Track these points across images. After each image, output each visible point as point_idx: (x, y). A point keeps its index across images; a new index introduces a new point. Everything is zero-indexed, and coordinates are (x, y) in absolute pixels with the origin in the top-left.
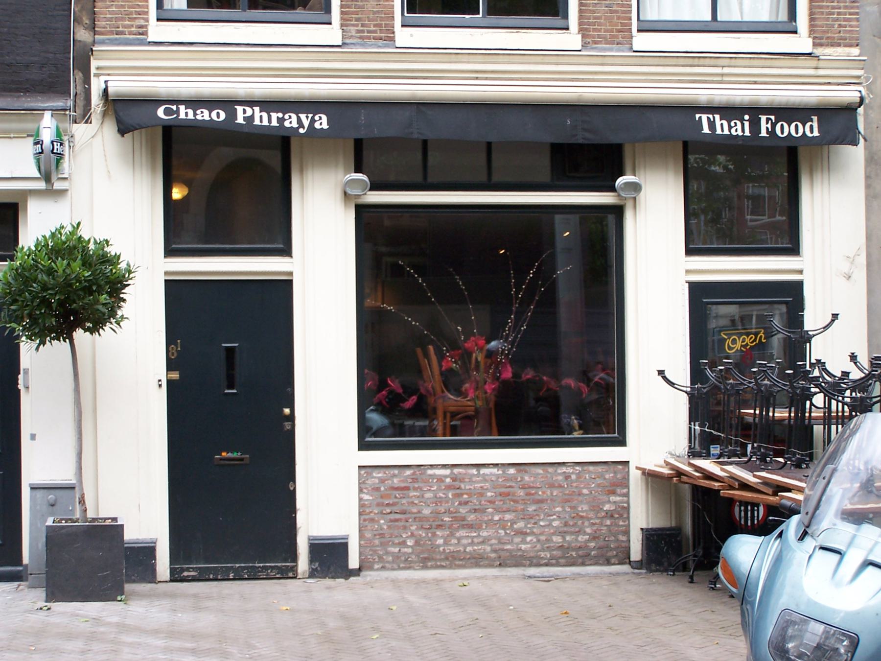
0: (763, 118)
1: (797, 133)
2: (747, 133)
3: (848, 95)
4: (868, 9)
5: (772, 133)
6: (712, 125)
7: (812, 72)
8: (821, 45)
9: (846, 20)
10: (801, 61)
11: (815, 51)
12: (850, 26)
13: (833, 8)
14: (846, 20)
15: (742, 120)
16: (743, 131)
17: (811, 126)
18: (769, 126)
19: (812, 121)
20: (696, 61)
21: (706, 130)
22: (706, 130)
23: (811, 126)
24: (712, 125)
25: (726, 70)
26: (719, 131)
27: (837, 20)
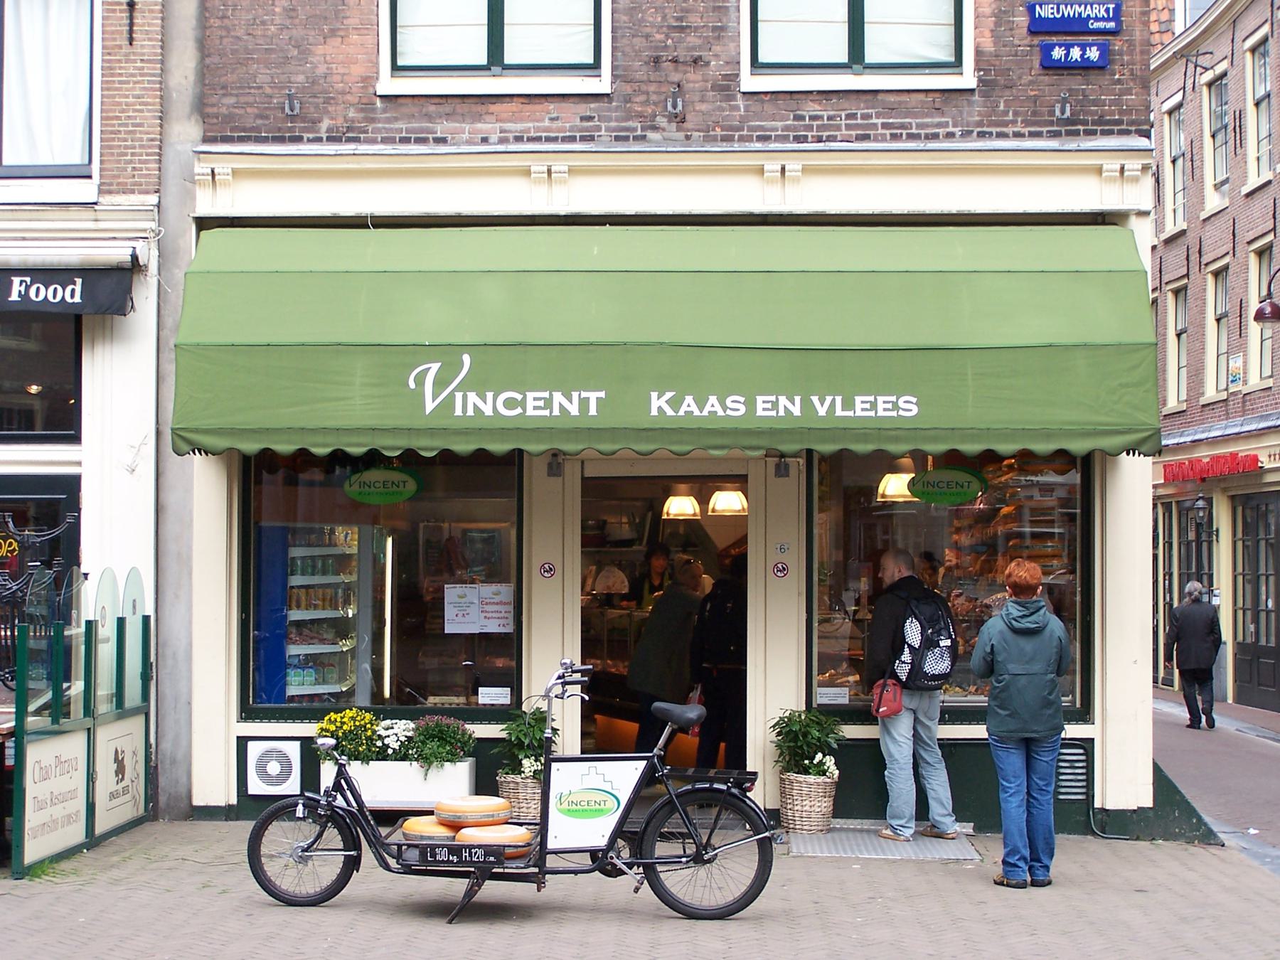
0: (16, 280)
1: (54, 297)
4: (179, 148)
5: (25, 296)
7: (91, 225)
8: (110, 192)
9: (141, 162)
10: (74, 213)
11: (101, 200)
12: (147, 169)
13: (126, 147)
14: (141, 162)
17: (73, 291)
18: (23, 289)
19: (74, 283)
23: (73, 291)
27: (131, 162)
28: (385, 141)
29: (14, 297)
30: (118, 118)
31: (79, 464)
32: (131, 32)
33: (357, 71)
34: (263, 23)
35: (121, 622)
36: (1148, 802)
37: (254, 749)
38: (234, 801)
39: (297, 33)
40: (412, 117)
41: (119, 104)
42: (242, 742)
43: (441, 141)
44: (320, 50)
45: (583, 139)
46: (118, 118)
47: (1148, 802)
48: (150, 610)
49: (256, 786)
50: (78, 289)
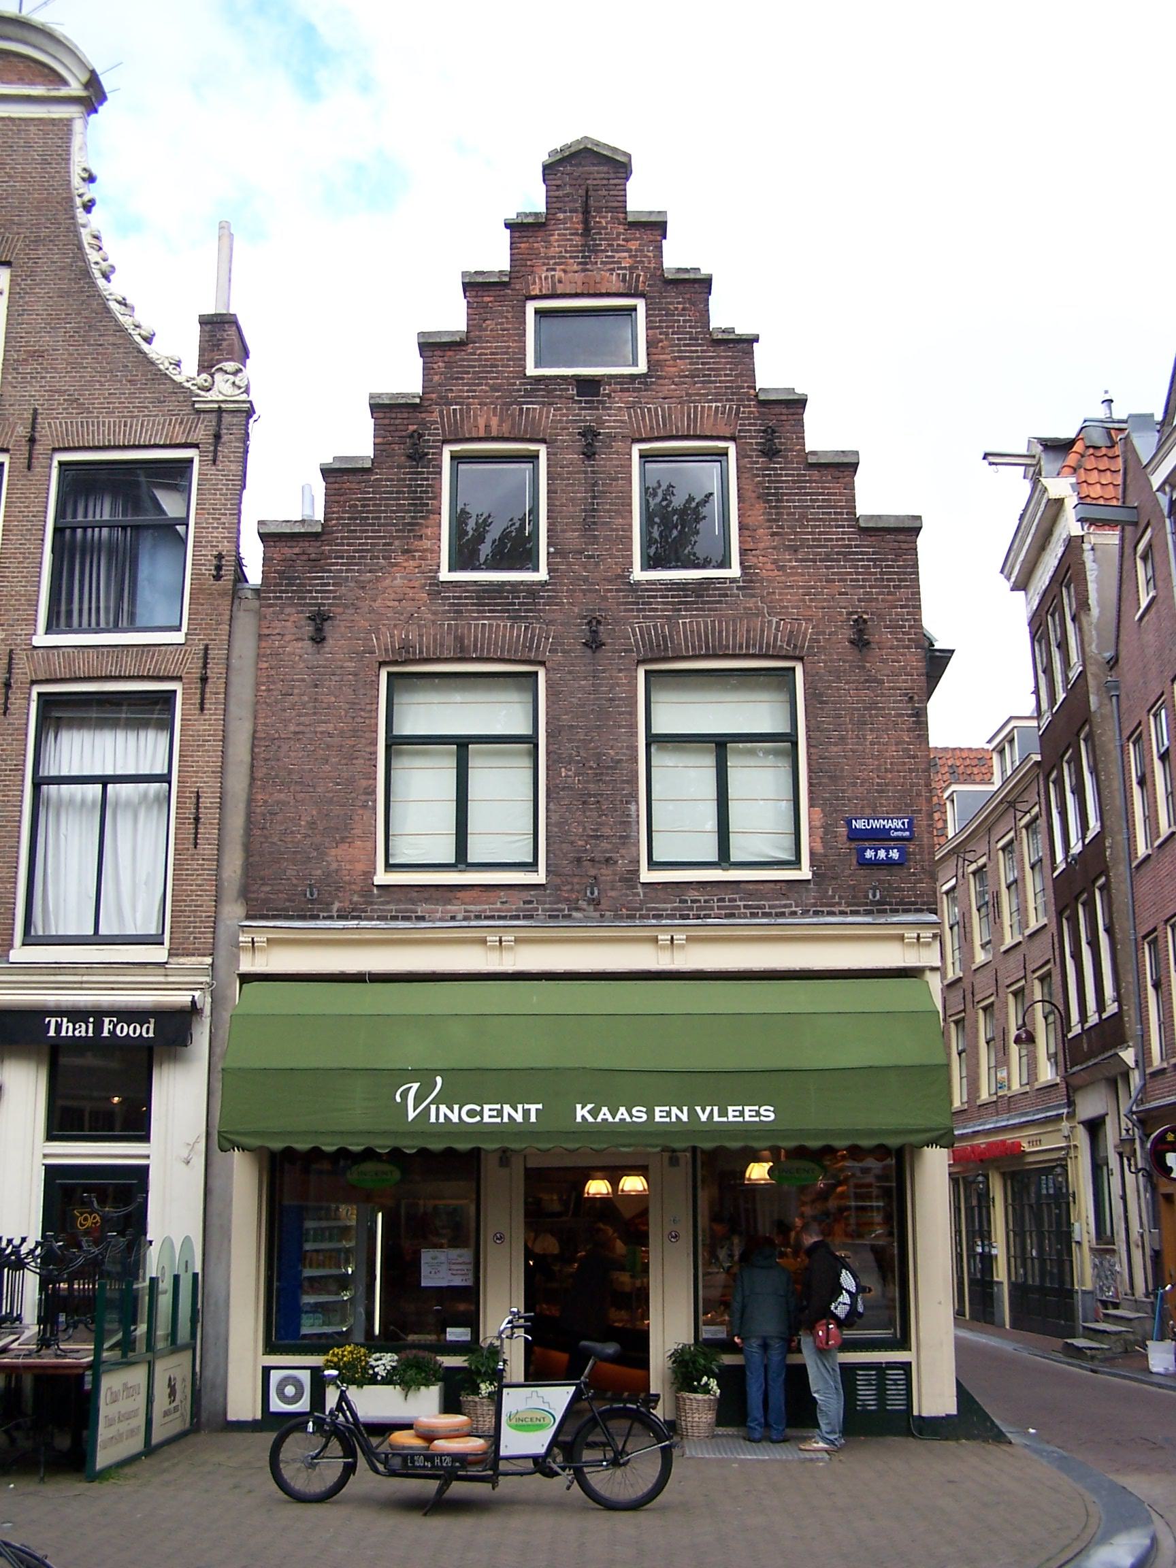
0: (107, 1020)
2: (90, 1034)
3: (182, 998)
6: (58, 1027)
8: (177, 955)
9: (200, 933)
14: (200, 933)
15: (87, 1023)
16: (87, 1032)
17: (148, 1028)
20: (58, 971)
21: (52, 1033)
22: (52, 1033)
23: (148, 1028)
24: (58, 1027)
25: (85, 978)
26: (63, 1034)
28: (379, 919)
29: (105, 1034)
30: (185, 901)
31: (148, 1157)
32: (196, 838)
33: (360, 867)
34: (292, 832)
35: (176, 1278)
36: (953, 1410)
37: (275, 1376)
38: (259, 1416)
39: (318, 839)
40: (399, 901)
41: (186, 890)
42: (266, 1371)
43: (422, 918)
44: (333, 852)
45: (525, 917)
46: (185, 901)
47: (953, 1410)
48: (198, 1269)
49: (277, 1405)
50: (152, 1026)
